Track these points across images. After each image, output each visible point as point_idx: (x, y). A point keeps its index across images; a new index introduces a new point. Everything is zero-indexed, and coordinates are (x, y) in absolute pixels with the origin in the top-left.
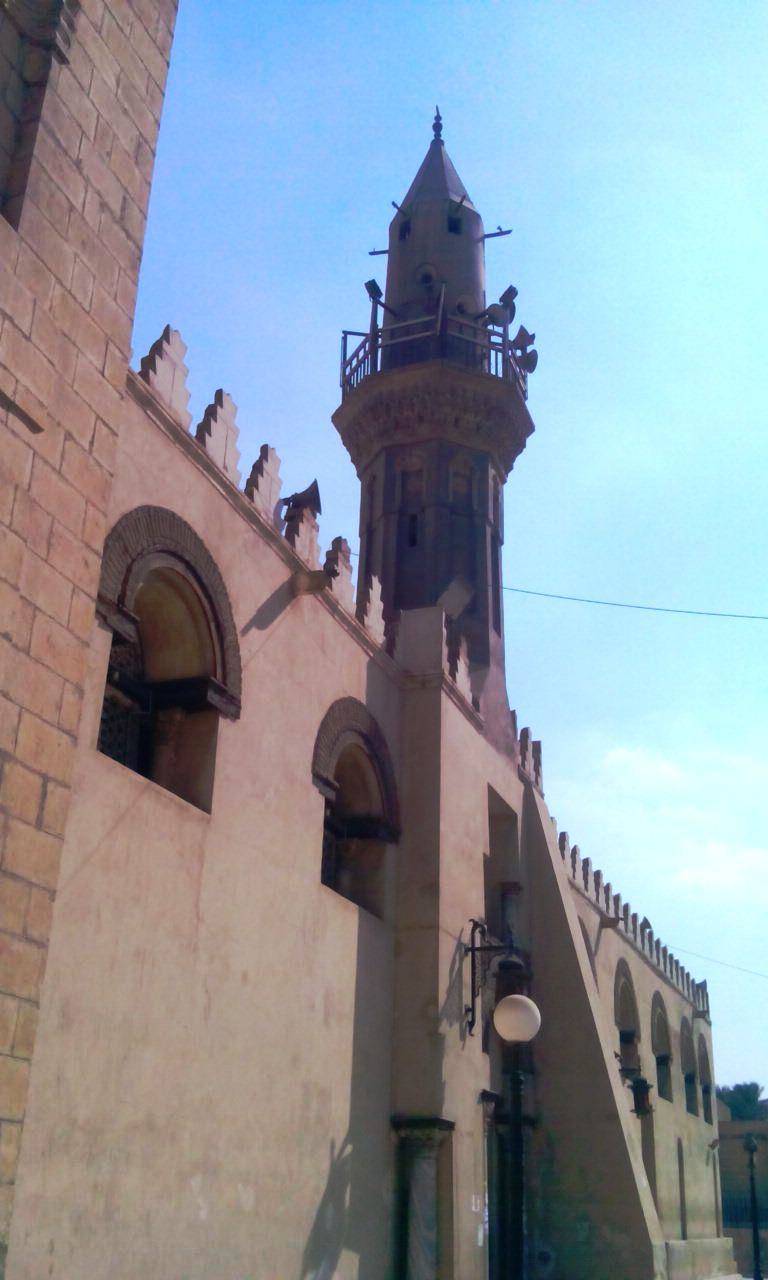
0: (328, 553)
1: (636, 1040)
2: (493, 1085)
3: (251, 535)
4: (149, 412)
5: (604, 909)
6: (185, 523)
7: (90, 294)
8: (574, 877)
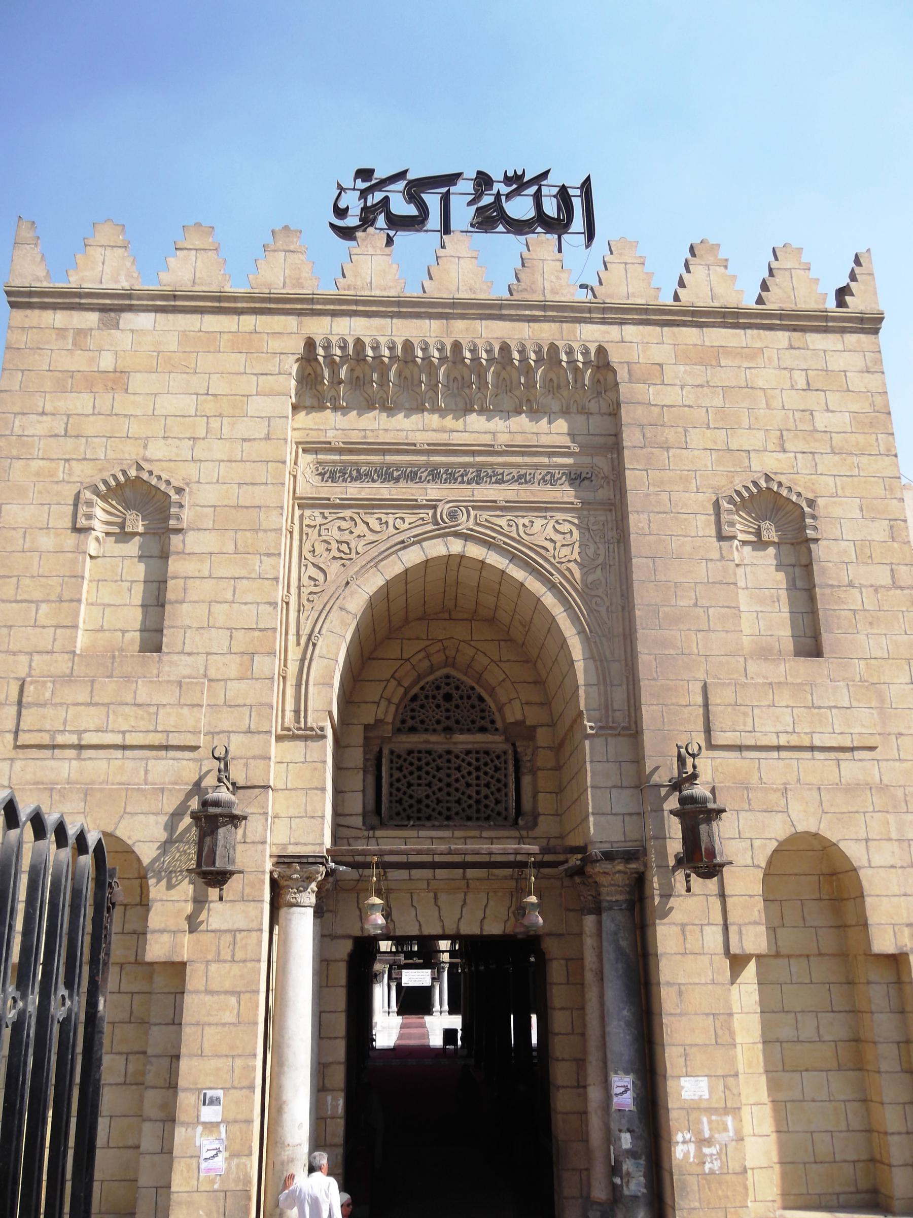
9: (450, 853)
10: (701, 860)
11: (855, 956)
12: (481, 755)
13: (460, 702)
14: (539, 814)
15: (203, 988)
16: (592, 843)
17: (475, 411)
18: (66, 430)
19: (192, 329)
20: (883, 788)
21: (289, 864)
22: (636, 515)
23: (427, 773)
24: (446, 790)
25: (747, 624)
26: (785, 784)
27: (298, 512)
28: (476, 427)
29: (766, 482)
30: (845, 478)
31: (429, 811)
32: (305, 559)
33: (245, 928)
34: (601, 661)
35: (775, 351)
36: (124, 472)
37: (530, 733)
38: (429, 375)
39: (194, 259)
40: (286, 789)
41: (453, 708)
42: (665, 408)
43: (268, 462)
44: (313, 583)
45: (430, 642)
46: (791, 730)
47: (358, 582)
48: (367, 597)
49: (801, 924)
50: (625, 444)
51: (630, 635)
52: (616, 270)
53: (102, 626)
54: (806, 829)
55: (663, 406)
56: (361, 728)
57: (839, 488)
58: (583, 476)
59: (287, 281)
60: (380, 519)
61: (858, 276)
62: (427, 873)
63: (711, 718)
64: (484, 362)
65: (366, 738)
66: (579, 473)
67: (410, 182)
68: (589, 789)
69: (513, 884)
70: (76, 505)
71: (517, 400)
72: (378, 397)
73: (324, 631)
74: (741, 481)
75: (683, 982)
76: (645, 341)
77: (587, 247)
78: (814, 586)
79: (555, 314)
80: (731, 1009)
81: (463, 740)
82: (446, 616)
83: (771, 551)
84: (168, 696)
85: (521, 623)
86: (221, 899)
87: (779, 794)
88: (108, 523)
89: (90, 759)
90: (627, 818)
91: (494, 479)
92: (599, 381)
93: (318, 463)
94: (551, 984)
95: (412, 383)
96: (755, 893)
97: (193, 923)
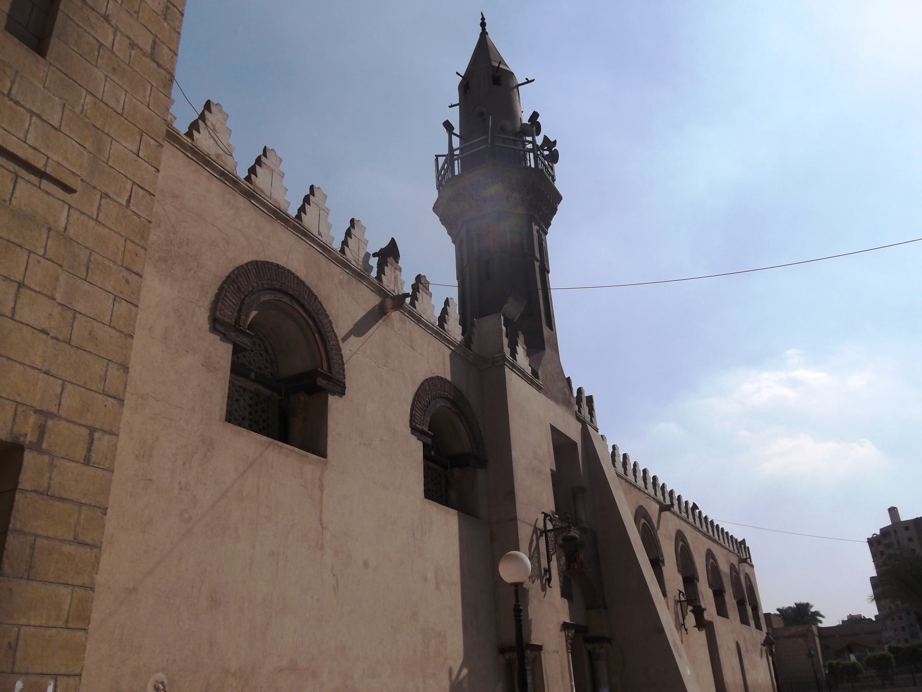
0: (413, 286)
1: (695, 581)
2: (572, 617)
3: (346, 276)
4: (252, 201)
5: (662, 500)
6: (288, 271)
7: (122, 103)
8: (636, 481)
20: (64, 236)
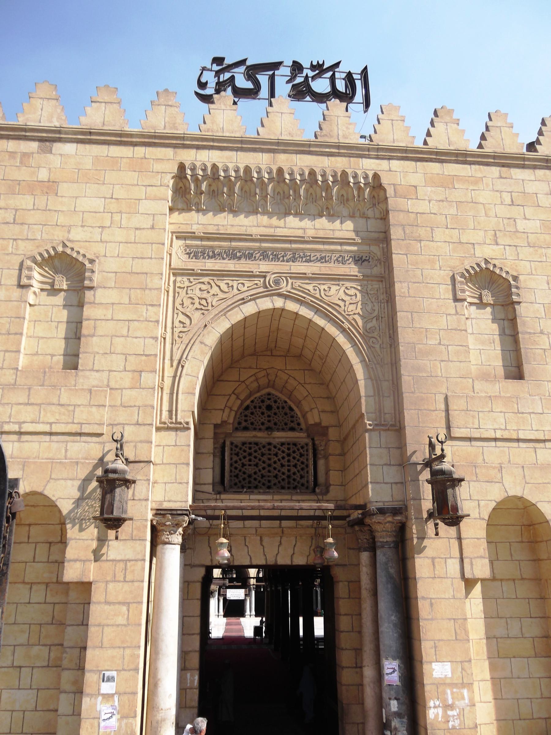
9: (274, 508)
10: (449, 513)
11: (546, 580)
12: (291, 446)
13: (277, 411)
14: (330, 485)
15: (104, 600)
16: (370, 502)
17: (292, 214)
18: (14, 220)
19: (102, 155)
21: (164, 515)
22: (399, 284)
23: (255, 457)
24: (267, 469)
25: (473, 357)
26: (500, 464)
27: (172, 278)
28: (293, 225)
29: (485, 264)
30: (537, 263)
31: (256, 483)
32: (177, 309)
33: (133, 558)
34: (376, 380)
35: (491, 179)
36: (54, 249)
37: (323, 431)
38: (261, 190)
39: (104, 108)
40: (163, 464)
41: (273, 415)
42: (418, 215)
43: (152, 244)
44: (182, 325)
45: (259, 370)
46: (503, 427)
47: (213, 325)
48: (219, 335)
49: (509, 558)
50: (392, 237)
51: (396, 364)
52: (386, 124)
53: (37, 352)
54: (515, 494)
55: (417, 213)
56: (212, 427)
57: (533, 269)
58: (364, 258)
59: (167, 125)
60: (228, 284)
61: (544, 133)
62: (255, 523)
63: (451, 419)
64: (298, 182)
65: (215, 434)
66: (360, 256)
67: (248, 67)
68: (369, 466)
69: (313, 531)
70: (20, 270)
71: (319, 208)
72: (227, 204)
73: (189, 357)
74: (469, 264)
75: (434, 597)
76: (405, 171)
77: (365, 112)
78: (518, 333)
79: (346, 151)
80: (466, 616)
81: (280, 436)
82: (269, 353)
83: (489, 309)
84: (82, 399)
85: (319, 356)
86: (117, 538)
87: (497, 470)
88: (42, 283)
89: (27, 441)
90: (394, 486)
91: (304, 259)
92: (374, 197)
93: (186, 246)
94: (338, 598)
95: (250, 195)
96: (481, 537)
97: (97, 555)
